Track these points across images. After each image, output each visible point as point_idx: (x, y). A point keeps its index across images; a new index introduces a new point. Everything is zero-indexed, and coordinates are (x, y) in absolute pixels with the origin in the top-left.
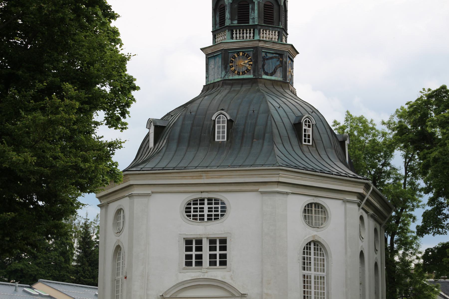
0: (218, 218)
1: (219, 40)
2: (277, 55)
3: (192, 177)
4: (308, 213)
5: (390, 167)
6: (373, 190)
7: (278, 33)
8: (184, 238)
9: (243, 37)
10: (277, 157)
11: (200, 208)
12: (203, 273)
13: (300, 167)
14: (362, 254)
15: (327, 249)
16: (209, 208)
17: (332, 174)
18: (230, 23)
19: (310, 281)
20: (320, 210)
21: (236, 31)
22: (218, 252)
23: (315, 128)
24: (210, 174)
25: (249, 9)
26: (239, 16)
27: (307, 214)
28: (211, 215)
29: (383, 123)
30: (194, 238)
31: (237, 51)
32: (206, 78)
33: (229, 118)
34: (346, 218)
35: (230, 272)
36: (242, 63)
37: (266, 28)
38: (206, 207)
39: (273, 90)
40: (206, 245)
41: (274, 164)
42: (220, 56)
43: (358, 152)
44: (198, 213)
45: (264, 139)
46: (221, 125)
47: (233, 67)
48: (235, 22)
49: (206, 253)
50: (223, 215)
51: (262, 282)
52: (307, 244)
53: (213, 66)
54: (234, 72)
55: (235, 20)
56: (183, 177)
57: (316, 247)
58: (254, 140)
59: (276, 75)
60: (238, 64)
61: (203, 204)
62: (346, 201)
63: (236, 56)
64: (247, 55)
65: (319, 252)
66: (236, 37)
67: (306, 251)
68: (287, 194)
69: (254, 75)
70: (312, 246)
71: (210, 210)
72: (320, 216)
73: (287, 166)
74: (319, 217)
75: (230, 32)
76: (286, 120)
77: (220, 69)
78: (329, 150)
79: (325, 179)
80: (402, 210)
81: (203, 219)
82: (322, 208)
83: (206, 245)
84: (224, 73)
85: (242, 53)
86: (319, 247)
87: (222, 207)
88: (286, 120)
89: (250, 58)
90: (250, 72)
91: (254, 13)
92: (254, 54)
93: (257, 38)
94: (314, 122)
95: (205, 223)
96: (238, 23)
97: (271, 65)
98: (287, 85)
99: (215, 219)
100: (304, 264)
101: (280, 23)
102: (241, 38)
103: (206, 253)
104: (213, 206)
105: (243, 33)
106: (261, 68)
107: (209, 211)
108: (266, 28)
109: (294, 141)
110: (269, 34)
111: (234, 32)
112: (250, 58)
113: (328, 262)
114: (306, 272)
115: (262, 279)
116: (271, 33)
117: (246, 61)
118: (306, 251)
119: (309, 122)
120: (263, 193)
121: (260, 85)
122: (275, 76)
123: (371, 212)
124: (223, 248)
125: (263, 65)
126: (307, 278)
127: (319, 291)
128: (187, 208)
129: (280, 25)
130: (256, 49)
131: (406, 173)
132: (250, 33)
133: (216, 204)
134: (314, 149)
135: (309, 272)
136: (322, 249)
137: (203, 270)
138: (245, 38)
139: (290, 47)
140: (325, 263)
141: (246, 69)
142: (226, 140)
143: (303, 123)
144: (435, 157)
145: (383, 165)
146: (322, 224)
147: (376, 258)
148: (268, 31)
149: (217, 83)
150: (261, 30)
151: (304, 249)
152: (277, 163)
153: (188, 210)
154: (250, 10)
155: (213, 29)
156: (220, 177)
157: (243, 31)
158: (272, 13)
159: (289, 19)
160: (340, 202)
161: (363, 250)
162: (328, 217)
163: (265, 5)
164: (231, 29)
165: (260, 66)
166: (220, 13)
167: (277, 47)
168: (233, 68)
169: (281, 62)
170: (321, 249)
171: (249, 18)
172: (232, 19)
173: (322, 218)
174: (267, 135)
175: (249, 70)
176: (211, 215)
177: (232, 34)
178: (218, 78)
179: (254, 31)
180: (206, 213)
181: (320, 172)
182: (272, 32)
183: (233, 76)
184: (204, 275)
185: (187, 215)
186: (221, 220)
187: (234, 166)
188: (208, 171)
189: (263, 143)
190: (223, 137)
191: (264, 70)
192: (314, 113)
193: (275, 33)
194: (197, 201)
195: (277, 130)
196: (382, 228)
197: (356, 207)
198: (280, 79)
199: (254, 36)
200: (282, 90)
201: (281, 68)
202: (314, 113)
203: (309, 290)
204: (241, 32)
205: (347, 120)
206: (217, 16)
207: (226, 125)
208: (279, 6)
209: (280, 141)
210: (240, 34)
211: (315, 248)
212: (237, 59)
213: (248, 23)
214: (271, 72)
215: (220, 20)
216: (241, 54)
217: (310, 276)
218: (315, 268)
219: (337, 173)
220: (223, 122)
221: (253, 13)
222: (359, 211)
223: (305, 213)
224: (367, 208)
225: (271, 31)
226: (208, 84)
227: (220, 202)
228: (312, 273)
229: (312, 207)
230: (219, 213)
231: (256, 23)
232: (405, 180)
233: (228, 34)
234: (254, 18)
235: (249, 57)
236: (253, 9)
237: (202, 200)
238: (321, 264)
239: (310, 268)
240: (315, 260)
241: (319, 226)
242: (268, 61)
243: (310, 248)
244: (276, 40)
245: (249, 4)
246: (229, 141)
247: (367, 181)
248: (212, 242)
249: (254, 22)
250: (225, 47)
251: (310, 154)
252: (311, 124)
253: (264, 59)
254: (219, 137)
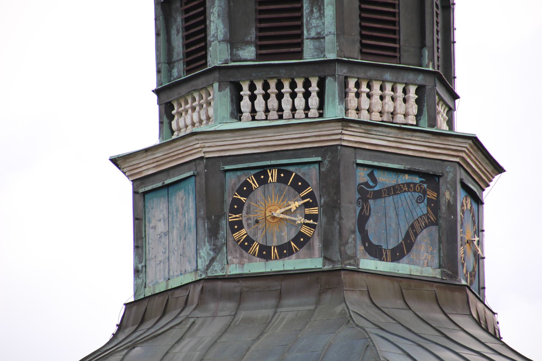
7: (416, 93)
26: (260, 30)
53: (161, 227)
77: (192, 237)
84: (206, 251)
85: (275, 172)
91: (322, 15)
111: (245, 92)
125: (363, 220)
129: (427, 61)
132: (307, 95)
141: (293, 235)
150: (352, 83)
155: (159, 82)
171: (301, 35)
179: (321, 85)
204: (273, 89)
210: (266, 97)
221: (316, 15)
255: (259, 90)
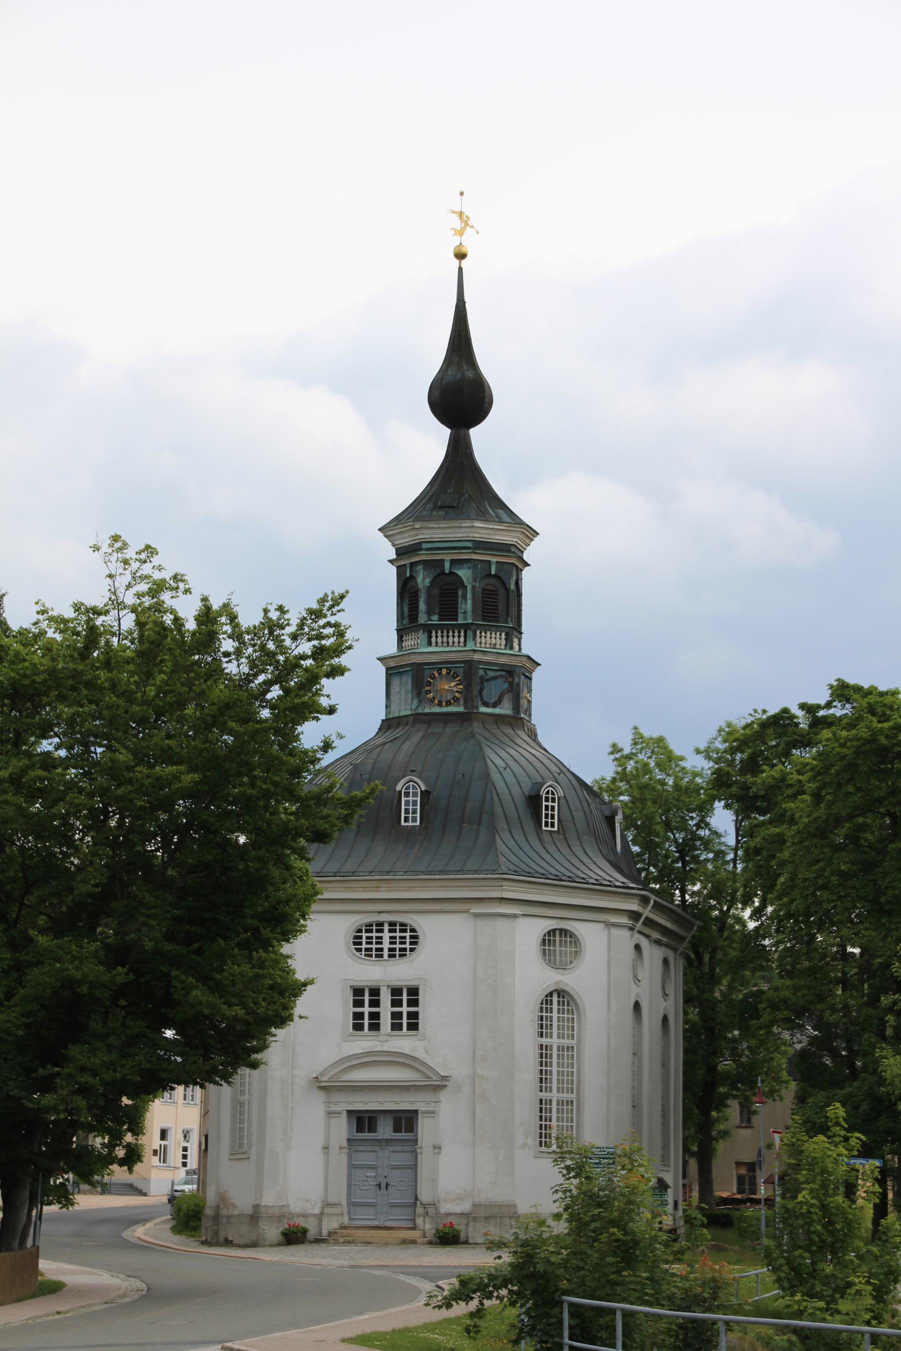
0: (406, 955)
1: (408, 643)
2: (504, 673)
3: (365, 889)
4: (549, 945)
5: (710, 829)
6: (655, 901)
8: (351, 986)
9: (448, 642)
10: (500, 856)
11: (377, 938)
12: (381, 1042)
13: (538, 872)
14: (637, 1006)
15: (579, 1003)
16: (391, 938)
17: (587, 883)
18: (426, 619)
19: (551, 1055)
20: (568, 939)
21: (437, 633)
22: (405, 1009)
23: (562, 801)
24: (393, 885)
25: (457, 597)
26: (440, 608)
27: (547, 948)
28: (394, 950)
29: (698, 751)
30: (367, 986)
31: (437, 666)
32: (387, 706)
33: (423, 789)
34: (609, 951)
35: (423, 1040)
36: (446, 687)
37: (486, 628)
38: (386, 935)
39: (497, 732)
40: (386, 998)
41: (494, 871)
42: (410, 673)
43: (651, 808)
44: (374, 946)
45: (479, 824)
46: (411, 799)
47: (430, 692)
48: (435, 617)
49: (386, 1009)
50: (415, 948)
51: (474, 1057)
52: (547, 996)
53: (397, 689)
54: (432, 701)
55: (435, 614)
56: (351, 889)
57: (561, 999)
58: (464, 825)
59: (501, 705)
60: (439, 689)
61: (382, 931)
62: (609, 925)
63: (437, 675)
64: (454, 673)
65: (566, 1007)
66: (437, 643)
67: (544, 1006)
68: (515, 916)
69: (466, 708)
70: (555, 999)
71: (393, 941)
72: (568, 949)
73: (516, 873)
74: (566, 951)
75: (426, 634)
76: (516, 790)
77: (410, 696)
78: (585, 838)
79: (576, 891)
80: (729, 909)
81: (381, 956)
82: (571, 937)
83: (386, 998)
84: (415, 702)
85: (445, 670)
86: (566, 1000)
87: (411, 937)
88: (516, 790)
89: (459, 678)
90: (459, 702)
91: (466, 603)
92: (465, 673)
93: (470, 646)
94: (561, 794)
95: (384, 962)
96: (440, 620)
97: (493, 690)
98: (519, 722)
99: (400, 956)
100: (542, 1028)
101: (509, 619)
102: (445, 644)
103: (386, 1009)
104: (398, 934)
105: (448, 637)
106: (477, 696)
107: (391, 943)
108: (485, 628)
109: (529, 825)
110: (491, 638)
111: (434, 634)
112: (459, 678)
113: (579, 1024)
114: (545, 1041)
115: (474, 1052)
116: (493, 635)
117: (453, 684)
118: (544, 1006)
119: (553, 794)
120: (476, 915)
121: (475, 724)
122: (501, 708)
123: (656, 935)
124: (413, 1003)
125: (481, 691)
126: (546, 1050)
127: (565, 1069)
128: (356, 937)
130: (470, 666)
131: (738, 841)
132: (459, 637)
133: (401, 931)
134: (561, 837)
135: (548, 1040)
136: (571, 1002)
137: (381, 1038)
138: (451, 644)
139: (524, 659)
140: (575, 1025)
141: (452, 697)
142: (418, 823)
143: (544, 795)
144: (755, 847)
145: (698, 826)
146: (571, 962)
147: (665, 1008)
148: (488, 633)
149: (404, 719)
150: (478, 632)
151: (542, 1003)
152: (499, 868)
153: (357, 941)
154: (460, 599)
155: (398, 626)
156: (409, 889)
157: (448, 632)
158: (496, 602)
159: (524, 608)
160: (601, 925)
161: (639, 1000)
162: (581, 951)
163: (484, 590)
164: (428, 629)
165: (476, 692)
166: (410, 601)
167: (503, 660)
168: (431, 694)
169: (511, 684)
170: (568, 1002)
171: (457, 611)
172: (429, 613)
173: (571, 952)
174: (484, 817)
175: (458, 699)
176: (394, 950)
177: (430, 637)
178: (406, 710)
179: (465, 633)
180: (386, 945)
181: (569, 881)
182: (496, 634)
183: (430, 708)
184: (383, 1045)
185: (355, 949)
186: (410, 956)
187: (430, 873)
188: (389, 880)
189: (478, 830)
190: (414, 820)
191: (482, 699)
192: (562, 775)
193: (500, 635)
194: (372, 925)
195: (501, 809)
196: (678, 957)
197: (626, 933)
198: (509, 712)
199: (465, 642)
200: (512, 732)
201: (511, 694)
202: (562, 775)
203: (548, 1068)
204: (445, 634)
205: (635, 744)
206: (404, 605)
207: (419, 799)
208: (507, 590)
209: (506, 827)
210: (442, 637)
211: (559, 1002)
212: (438, 679)
213: (456, 620)
214: (493, 701)
215: (410, 612)
216: (444, 672)
217: (551, 1046)
218: (559, 1034)
219: (596, 880)
220: (415, 795)
222: (631, 938)
223: (544, 945)
224: (647, 931)
225: (493, 633)
226: (389, 719)
227: (408, 928)
228: (555, 1041)
229: (554, 936)
230: (408, 946)
231: (470, 621)
232: (736, 854)
233: (422, 636)
234: (465, 613)
235: (458, 676)
236: (464, 597)
237: (380, 924)
238: (568, 1027)
239: (551, 1033)
240: (559, 1021)
241: (566, 965)
242: (489, 683)
243: (551, 1001)
244: (503, 647)
245: (457, 589)
246: (423, 825)
247: (643, 892)
248: (396, 992)
249: (465, 618)
250: (419, 659)
251: (554, 846)
252: (556, 796)
253: (483, 680)
254: (406, 820)
255: (439, 634)
